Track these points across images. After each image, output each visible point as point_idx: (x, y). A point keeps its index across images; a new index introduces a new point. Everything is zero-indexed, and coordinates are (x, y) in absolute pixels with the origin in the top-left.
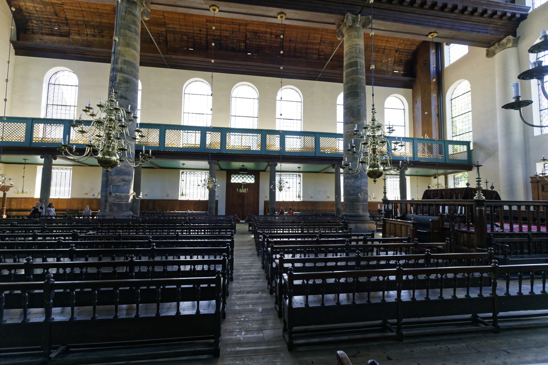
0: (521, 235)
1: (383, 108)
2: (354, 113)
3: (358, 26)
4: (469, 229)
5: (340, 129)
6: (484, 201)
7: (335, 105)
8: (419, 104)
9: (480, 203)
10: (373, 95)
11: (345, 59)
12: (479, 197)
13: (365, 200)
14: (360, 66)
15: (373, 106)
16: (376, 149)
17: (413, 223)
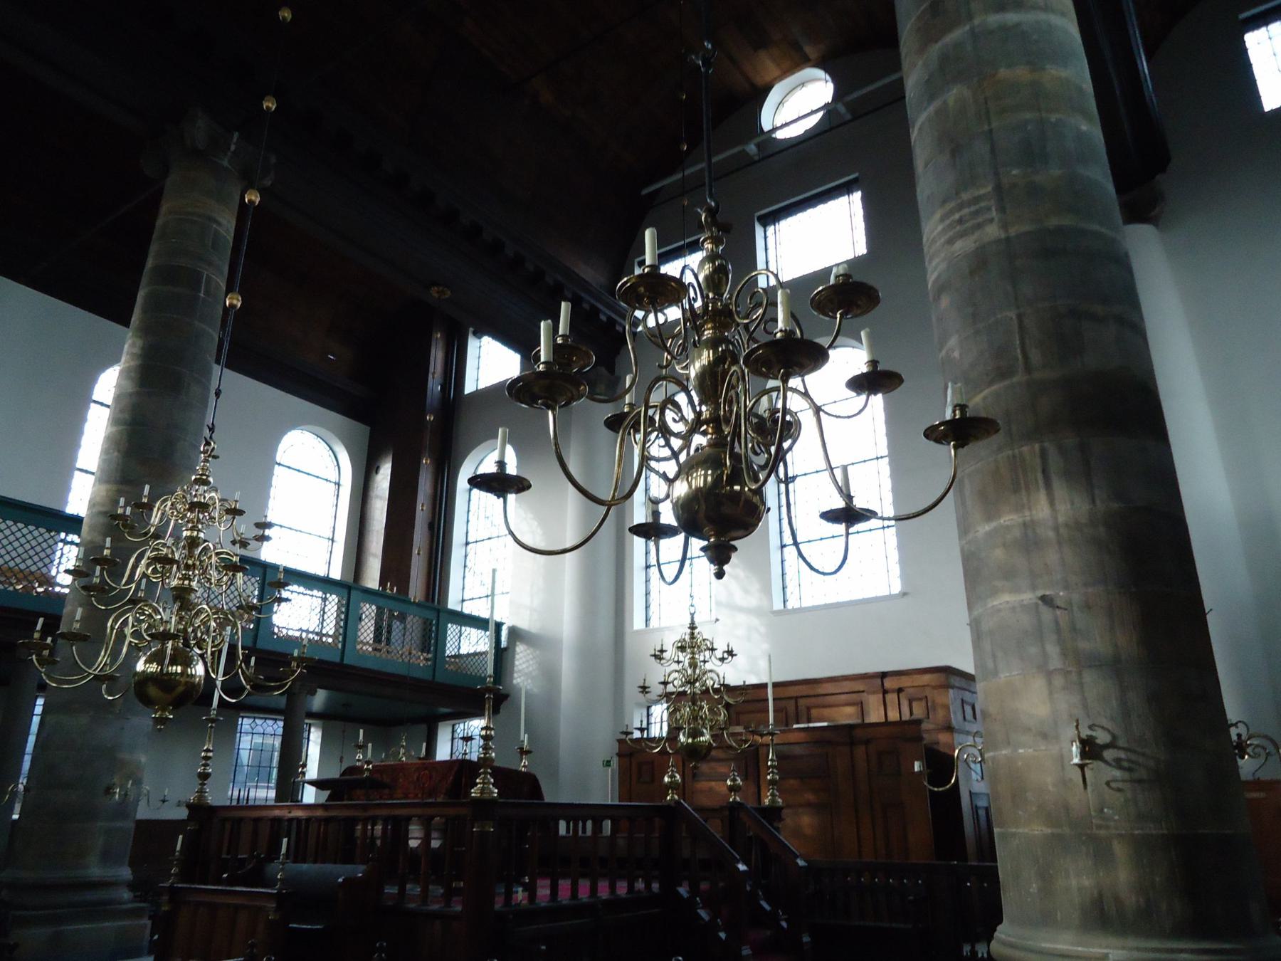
0: (577, 910)
1: (264, 464)
2: (150, 451)
3: (225, 163)
4: (448, 904)
5: (80, 497)
6: (493, 801)
7: (82, 399)
8: (383, 480)
9: (484, 805)
10: (218, 394)
11: (154, 248)
12: (482, 790)
13: (124, 809)
14: (207, 293)
15: (212, 429)
16: (191, 590)
17: (279, 897)
